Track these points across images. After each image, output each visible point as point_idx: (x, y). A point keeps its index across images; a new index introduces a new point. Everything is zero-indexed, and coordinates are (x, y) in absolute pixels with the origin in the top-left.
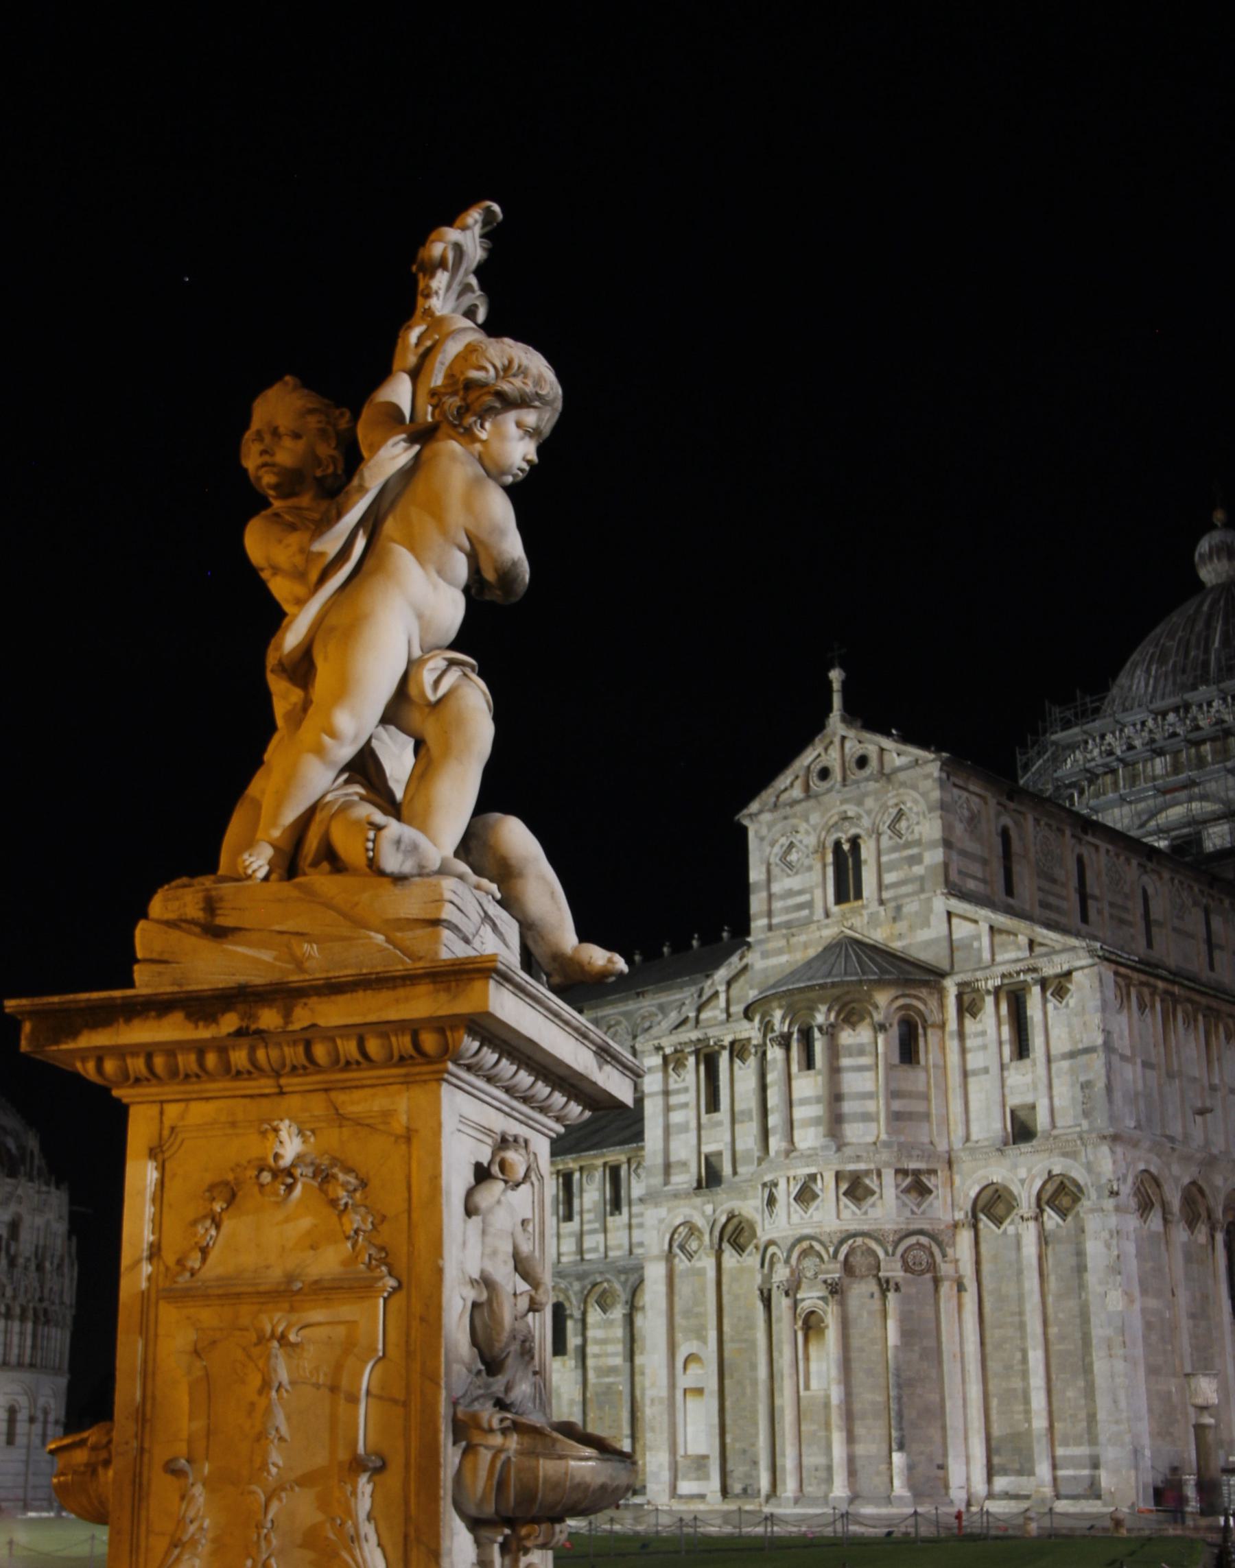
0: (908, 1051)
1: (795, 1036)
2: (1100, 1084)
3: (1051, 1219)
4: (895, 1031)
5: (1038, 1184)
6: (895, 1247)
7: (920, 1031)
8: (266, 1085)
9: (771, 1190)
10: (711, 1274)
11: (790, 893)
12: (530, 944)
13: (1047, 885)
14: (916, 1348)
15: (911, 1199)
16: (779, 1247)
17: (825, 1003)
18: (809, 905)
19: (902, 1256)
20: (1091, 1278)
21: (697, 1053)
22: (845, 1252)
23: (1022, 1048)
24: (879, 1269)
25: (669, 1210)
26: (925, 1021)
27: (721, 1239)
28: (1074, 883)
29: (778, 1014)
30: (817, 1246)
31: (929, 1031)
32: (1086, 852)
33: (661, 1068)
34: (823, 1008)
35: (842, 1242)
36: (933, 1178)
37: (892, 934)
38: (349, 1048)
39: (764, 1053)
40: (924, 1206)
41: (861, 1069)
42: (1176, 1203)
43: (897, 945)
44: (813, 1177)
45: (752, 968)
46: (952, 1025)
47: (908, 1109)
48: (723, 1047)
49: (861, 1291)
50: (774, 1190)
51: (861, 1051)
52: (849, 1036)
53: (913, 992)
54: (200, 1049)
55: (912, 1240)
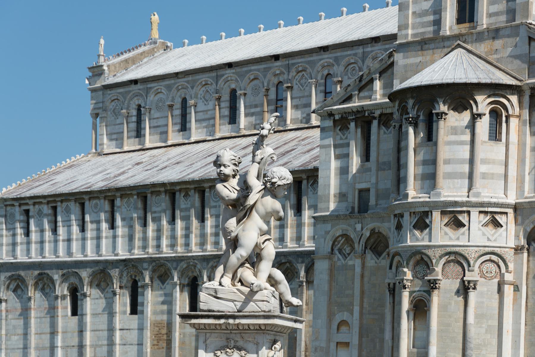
1: (421, 117)
6: (476, 261)
7: (504, 119)
8: (229, 332)
9: (399, 219)
10: (358, 270)
12: (281, 297)
14: (484, 326)
15: (490, 230)
16: (401, 257)
17: (442, 98)
19: (479, 267)
21: (356, 120)
22: (443, 263)
24: (464, 276)
25: (332, 227)
26: (507, 111)
27: (366, 248)
29: (411, 102)
30: (426, 259)
33: (333, 128)
35: (441, 257)
36: (504, 217)
37: (491, 49)
38: (247, 328)
39: (401, 126)
40: (497, 235)
41: (462, 143)
45: (397, 64)
47: (491, 172)
48: (375, 118)
50: (400, 219)
52: (457, 120)
53: (500, 92)
54: (216, 324)
55: (487, 257)
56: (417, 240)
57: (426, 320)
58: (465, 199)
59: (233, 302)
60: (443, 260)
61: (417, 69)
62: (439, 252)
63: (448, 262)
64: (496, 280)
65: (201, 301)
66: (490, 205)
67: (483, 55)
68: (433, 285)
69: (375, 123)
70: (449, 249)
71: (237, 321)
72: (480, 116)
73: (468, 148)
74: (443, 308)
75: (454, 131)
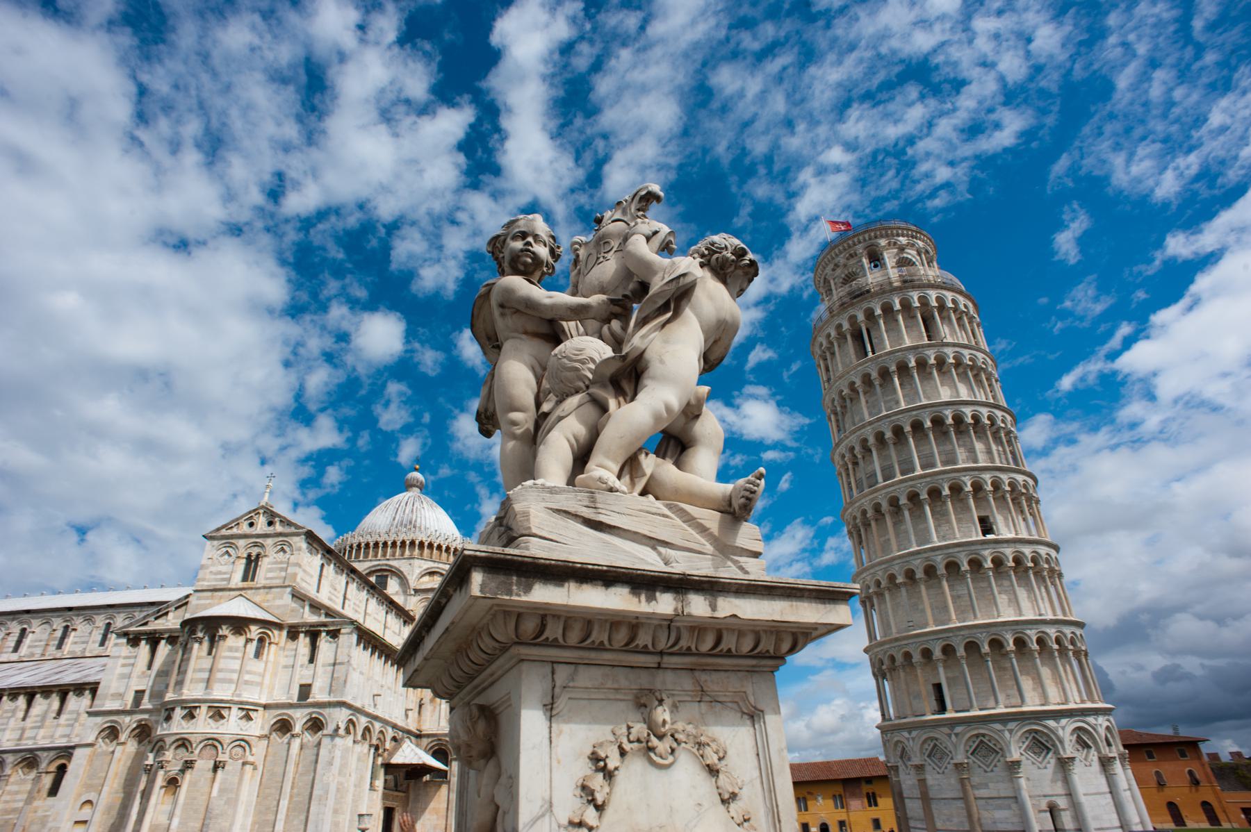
0: (258, 654)
2: (343, 679)
3: (308, 737)
4: (255, 643)
5: (305, 720)
8: (650, 660)
11: (220, 573)
13: (332, 591)
15: (244, 722)
18: (229, 580)
20: (319, 766)
23: (312, 660)
28: (343, 592)
29: (200, 627)
31: (273, 647)
32: (350, 580)
34: (224, 627)
35: (201, 742)
36: (255, 713)
39: (186, 644)
42: (360, 732)
43: (265, 605)
44: (196, 707)
46: (282, 644)
49: (203, 765)
51: (237, 650)
55: (237, 743)
56: (183, 728)
57: (174, 793)
58: (229, 698)
59: (654, 548)
60: (202, 744)
61: (211, 606)
62: (201, 737)
63: (206, 746)
64: (241, 761)
65: (534, 531)
66: (247, 703)
67: (258, 602)
68: (188, 765)
69: (163, 642)
70: (209, 736)
71: (728, 607)
72: (251, 640)
73: (239, 662)
74: (193, 784)
75: (231, 649)
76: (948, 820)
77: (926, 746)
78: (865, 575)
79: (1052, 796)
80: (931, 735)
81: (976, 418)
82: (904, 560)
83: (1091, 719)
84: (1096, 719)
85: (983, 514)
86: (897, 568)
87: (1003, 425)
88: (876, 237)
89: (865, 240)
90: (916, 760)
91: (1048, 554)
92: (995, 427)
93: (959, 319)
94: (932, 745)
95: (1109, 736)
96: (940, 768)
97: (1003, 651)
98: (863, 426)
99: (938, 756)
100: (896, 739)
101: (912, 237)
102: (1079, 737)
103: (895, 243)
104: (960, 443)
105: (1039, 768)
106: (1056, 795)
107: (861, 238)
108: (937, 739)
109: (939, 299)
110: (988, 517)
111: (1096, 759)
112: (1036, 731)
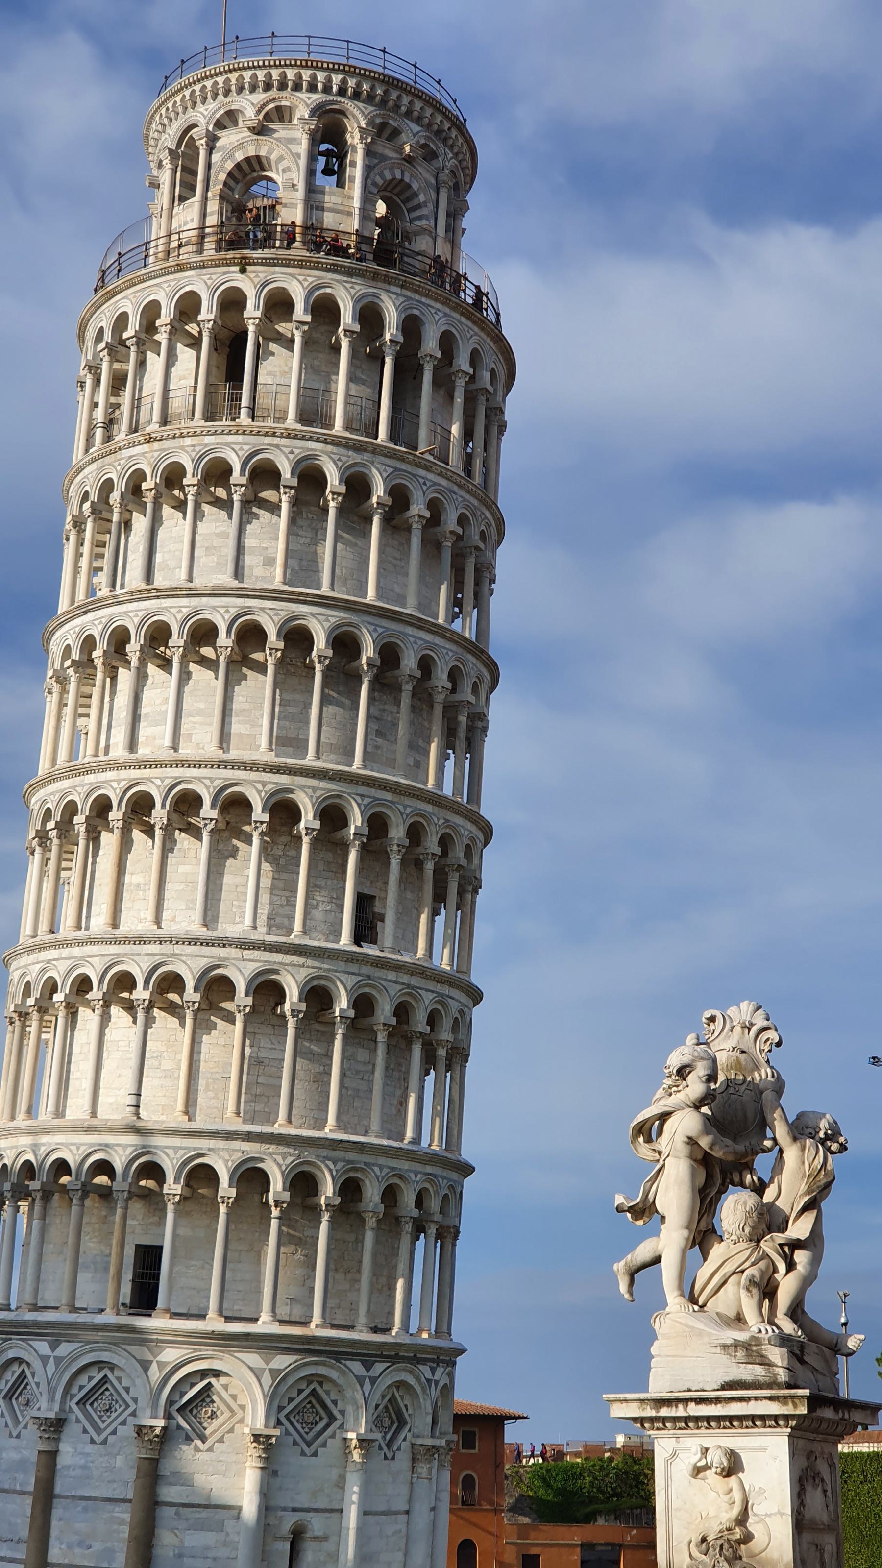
76: (80, 1544)
77: (83, 1380)
78: (53, 954)
79: (308, 1510)
80: (105, 1356)
81: (426, 664)
82: (167, 948)
83: (425, 1370)
84: (433, 1372)
85: (366, 891)
86: (146, 966)
87: (472, 699)
88: (357, 95)
89: (327, 89)
90: (46, 1409)
91: (461, 1012)
92: (457, 697)
93: (470, 400)
94: (98, 1377)
95: (439, 1404)
96: (99, 1431)
97: (311, 1201)
98: (172, 593)
99: (101, 1405)
100: (11, 1354)
101: (439, 132)
102: (393, 1401)
103: (396, 133)
104: (374, 711)
105: (303, 1454)
106: (316, 1510)
107: (321, 76)
108: (112, 1367)
109: (447, 341)
110: (372, 898)
111: (406, 1446)
112: (322, 1380)
